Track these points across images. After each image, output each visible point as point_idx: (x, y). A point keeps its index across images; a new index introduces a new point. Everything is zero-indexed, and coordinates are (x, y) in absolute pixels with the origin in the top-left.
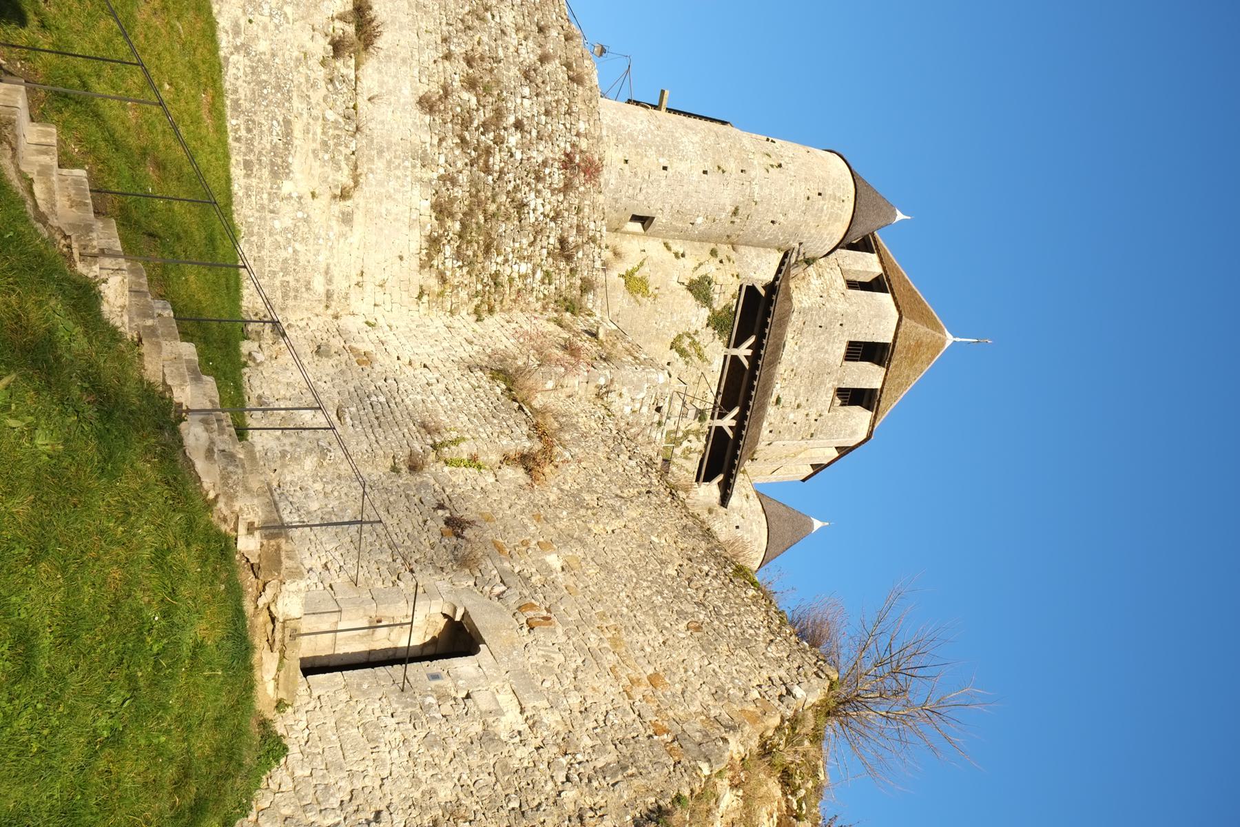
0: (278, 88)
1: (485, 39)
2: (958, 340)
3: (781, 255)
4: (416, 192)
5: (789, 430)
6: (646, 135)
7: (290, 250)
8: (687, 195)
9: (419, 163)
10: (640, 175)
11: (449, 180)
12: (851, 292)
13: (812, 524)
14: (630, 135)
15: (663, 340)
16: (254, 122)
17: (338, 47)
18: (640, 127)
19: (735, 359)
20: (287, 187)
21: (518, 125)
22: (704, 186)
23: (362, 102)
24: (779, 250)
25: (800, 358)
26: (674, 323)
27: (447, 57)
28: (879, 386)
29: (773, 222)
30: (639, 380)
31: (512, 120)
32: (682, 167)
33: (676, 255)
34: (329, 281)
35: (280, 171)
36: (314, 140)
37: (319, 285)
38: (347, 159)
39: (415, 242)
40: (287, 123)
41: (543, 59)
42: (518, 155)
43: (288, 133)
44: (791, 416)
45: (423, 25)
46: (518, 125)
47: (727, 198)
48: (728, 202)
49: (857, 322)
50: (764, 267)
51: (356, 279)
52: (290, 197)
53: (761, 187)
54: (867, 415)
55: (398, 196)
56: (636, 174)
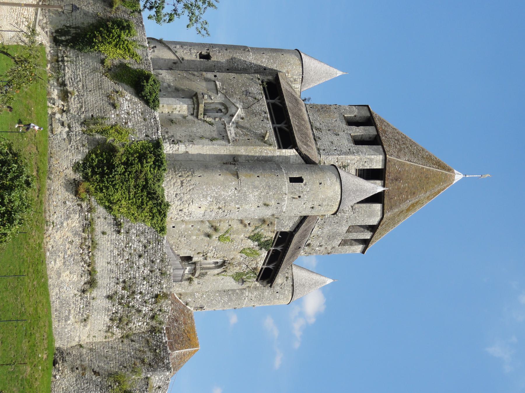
0: (68, 304)
10: (226, 211)
18: (230, 193)
20: (69, 322)
32: (247, 207)
33: (245, 226)
35: (67, 318)
45: (111, 276)
53: (287, 207)
56: (224, 211)
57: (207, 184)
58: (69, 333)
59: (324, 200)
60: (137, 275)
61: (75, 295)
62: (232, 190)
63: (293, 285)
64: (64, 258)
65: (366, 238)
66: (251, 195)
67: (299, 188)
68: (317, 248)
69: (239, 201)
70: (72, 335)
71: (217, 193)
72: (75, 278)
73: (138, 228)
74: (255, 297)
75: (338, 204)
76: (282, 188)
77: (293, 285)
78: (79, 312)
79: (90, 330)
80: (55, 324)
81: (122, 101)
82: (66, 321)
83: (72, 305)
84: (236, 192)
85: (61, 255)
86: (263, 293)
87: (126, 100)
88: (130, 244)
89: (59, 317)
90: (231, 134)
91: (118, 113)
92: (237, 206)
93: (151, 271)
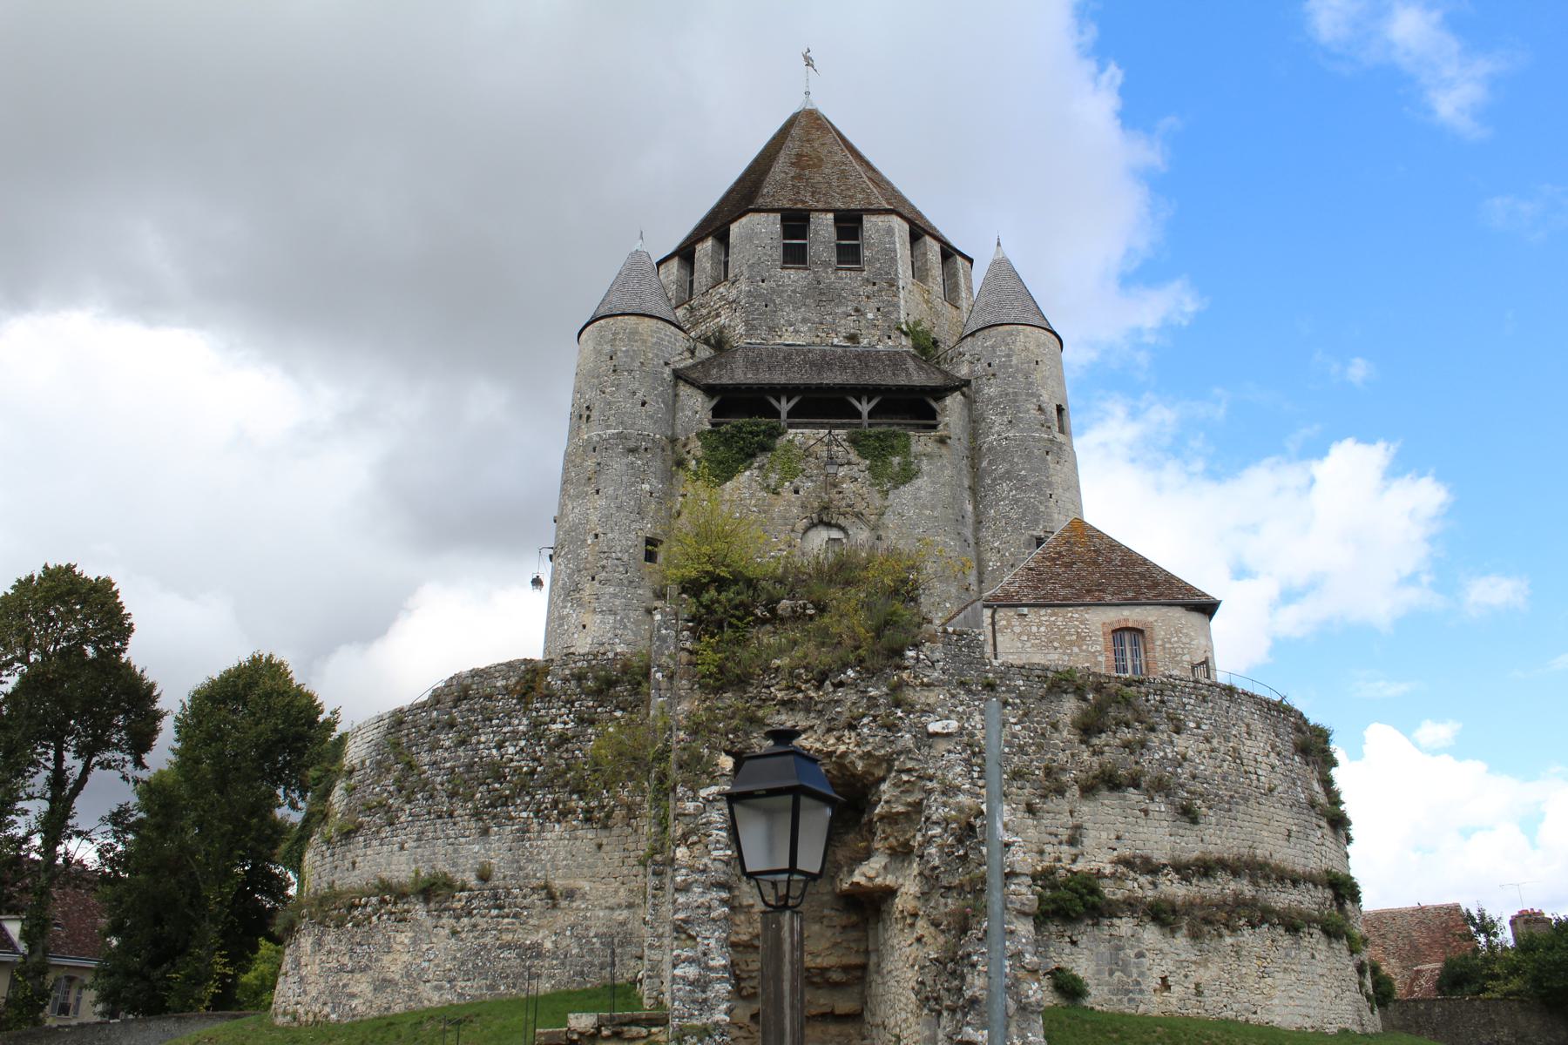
0: (477, 953)
1: (439, 779)
3: (681, 383)
4: (549, 836)
5: (885, 315)
8: (619, 508)
14: (570, 576)
15: (770, 505)
19: (790, 414)
21: (499, 746)
22: (611, 491)
24: (676, 385)
25: (804, 321)
26: (752, 496)
28: (831, 216)
29: (643, 404)
31: (494, 752)
32: (594, 518)
34: (620, 906)
35: (536, 951)
37: (621, 915)
39: (589, 835)
42: (523, 743)
43: (508, 946)
44: (870, 316)
46: (499, 746)
47: (618, 464)
48: (625, 461)
49: (759, 262)
53: (608, 427)
54: (869, 222)
55: (553, 850)
56: (604, 567)
58: (588, 942)
59: (599, 353)
61: (454, 933)
63: (972, 334)
64: (352, 971)
65: (831, 222)
68: (870, 316)
70: (601, 930)
72: (405, 938)
75: (611, 320)
77: (972, 334)
78: (516, 916)
79: (592, 878)
80: (545, 986)
82: (539, 955)
83: (488, 939)
85: (346, 977)
86: (991, 399)
89: (519, 976)
93: (451, 725)
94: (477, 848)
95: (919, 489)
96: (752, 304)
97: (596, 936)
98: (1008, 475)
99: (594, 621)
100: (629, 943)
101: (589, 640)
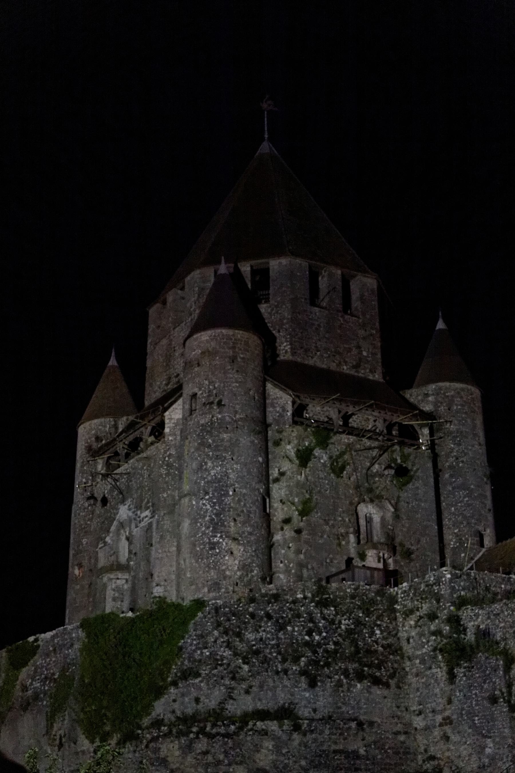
2: (266, 136)
6: (214, 503)
7: (389, 751)
9: (341, 689)
11: (346, 673)
12: (272, 302)
13: (440, 329)
16: (337, 767)
17: (297, 728)
18: (208, 507)
20: (362, 751)
21: (309, 633)
23: (318, 716)
25: (326, 349)
27: (286, 672)
30: (450, 588)
31: (307, 638)
35: (355, 755)
36: (339, 739)
38: (345, 724)
40: (335, 752)
41: (269, 616)
46: (309, 633)
50: (281, 402)
51: (396, 720)
52: (366, 751)
57: (195, 545)
58: (386, 752)
60: (273, 642)
62: (204, 504)
66: (213, 473)
67: (203, 397)
69: (223, 490)
70: (393, 745)
71: (208, 528)
73: (194, 648)
74: (459, 444)
76: (202, 425)
81: (31, 692)
84: (207, 497)
86: (452, 433)
87: (31, 684)
88: (218, 657)
90: (147, 516)
91: (42, 696)
92: (231, 493)
94: (307, 695)
95: (417, 488)
96: (294, 330)
97: (389, 748)
98: (463, 487)
99: (238, 550)
100: (408, 753)
101: (237, 562)
